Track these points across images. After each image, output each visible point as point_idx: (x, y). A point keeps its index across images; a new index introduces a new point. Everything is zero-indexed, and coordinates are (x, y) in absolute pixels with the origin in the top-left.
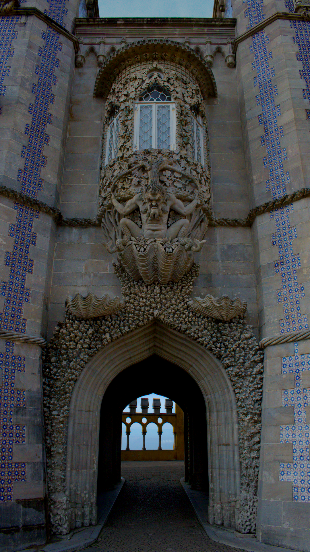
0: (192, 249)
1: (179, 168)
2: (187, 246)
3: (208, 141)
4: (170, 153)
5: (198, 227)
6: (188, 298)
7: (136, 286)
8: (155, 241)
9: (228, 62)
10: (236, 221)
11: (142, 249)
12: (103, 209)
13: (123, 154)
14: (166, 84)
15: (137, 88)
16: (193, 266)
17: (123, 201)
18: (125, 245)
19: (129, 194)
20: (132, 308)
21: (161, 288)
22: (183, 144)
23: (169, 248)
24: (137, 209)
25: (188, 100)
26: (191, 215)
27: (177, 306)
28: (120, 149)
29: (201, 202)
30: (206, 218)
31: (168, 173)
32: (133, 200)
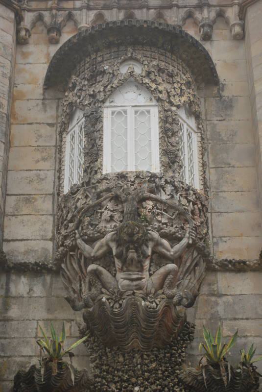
1: (164, 197)
2: (175, 300)
3: (203, 151)
4: (151, 177)
5: (190, 274)
6: (180, 370)
8: (134, 294)
10: (244, 263)
11: (117, 305)
12: (64, 252)
13: (90, 178)
14: (146, 81)
15: (107, 86)
16: (186, 326)
17: (91, 241)
18: (93, 300)
19: (99, 232)
20: (104, 384)
21: (142, 357)
22: (169, 163)
23: (152, 302)
24: (110, 251)
25: (175, 100)
26: (180, 257)
27: (165, 380)
28: (85, 171)
29: (194, 240)
30: (202, 260)
31: (149, 204)
32: (103, 240)
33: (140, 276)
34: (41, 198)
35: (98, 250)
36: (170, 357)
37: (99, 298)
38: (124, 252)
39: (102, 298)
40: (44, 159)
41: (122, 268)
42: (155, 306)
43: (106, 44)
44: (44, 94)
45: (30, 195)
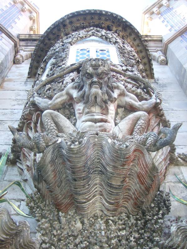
0: (158, 144)
2: (150, 140)
7: (63, 220)
8: (97, 134)
9: (160, 59)
11: (77, 143)
21: (107, 222)
33: (104, 117)
34: (11, 122)
35: (56, 99)
36: (144, 226)
37: (55, 140)
38: (87, 90)
39: (58, 140)
40: (18, 104)
41: (83, 110)
42: (125, 146)
43: (75, 27)
44: (27, 80)
45: (2, 121)
